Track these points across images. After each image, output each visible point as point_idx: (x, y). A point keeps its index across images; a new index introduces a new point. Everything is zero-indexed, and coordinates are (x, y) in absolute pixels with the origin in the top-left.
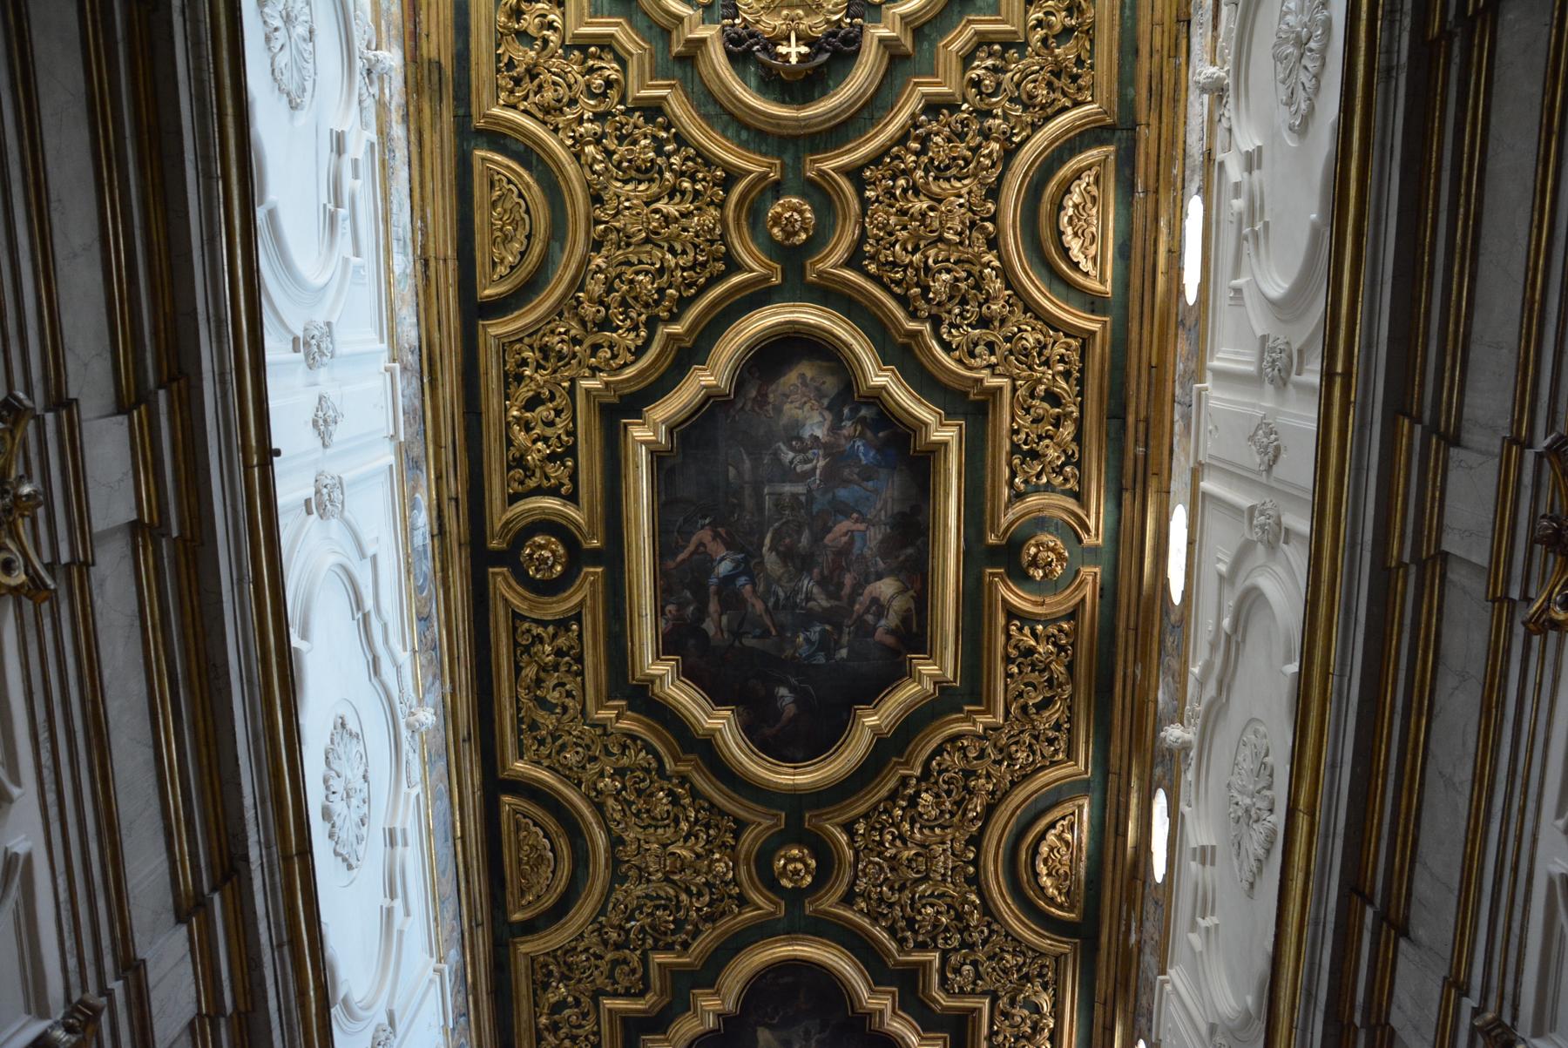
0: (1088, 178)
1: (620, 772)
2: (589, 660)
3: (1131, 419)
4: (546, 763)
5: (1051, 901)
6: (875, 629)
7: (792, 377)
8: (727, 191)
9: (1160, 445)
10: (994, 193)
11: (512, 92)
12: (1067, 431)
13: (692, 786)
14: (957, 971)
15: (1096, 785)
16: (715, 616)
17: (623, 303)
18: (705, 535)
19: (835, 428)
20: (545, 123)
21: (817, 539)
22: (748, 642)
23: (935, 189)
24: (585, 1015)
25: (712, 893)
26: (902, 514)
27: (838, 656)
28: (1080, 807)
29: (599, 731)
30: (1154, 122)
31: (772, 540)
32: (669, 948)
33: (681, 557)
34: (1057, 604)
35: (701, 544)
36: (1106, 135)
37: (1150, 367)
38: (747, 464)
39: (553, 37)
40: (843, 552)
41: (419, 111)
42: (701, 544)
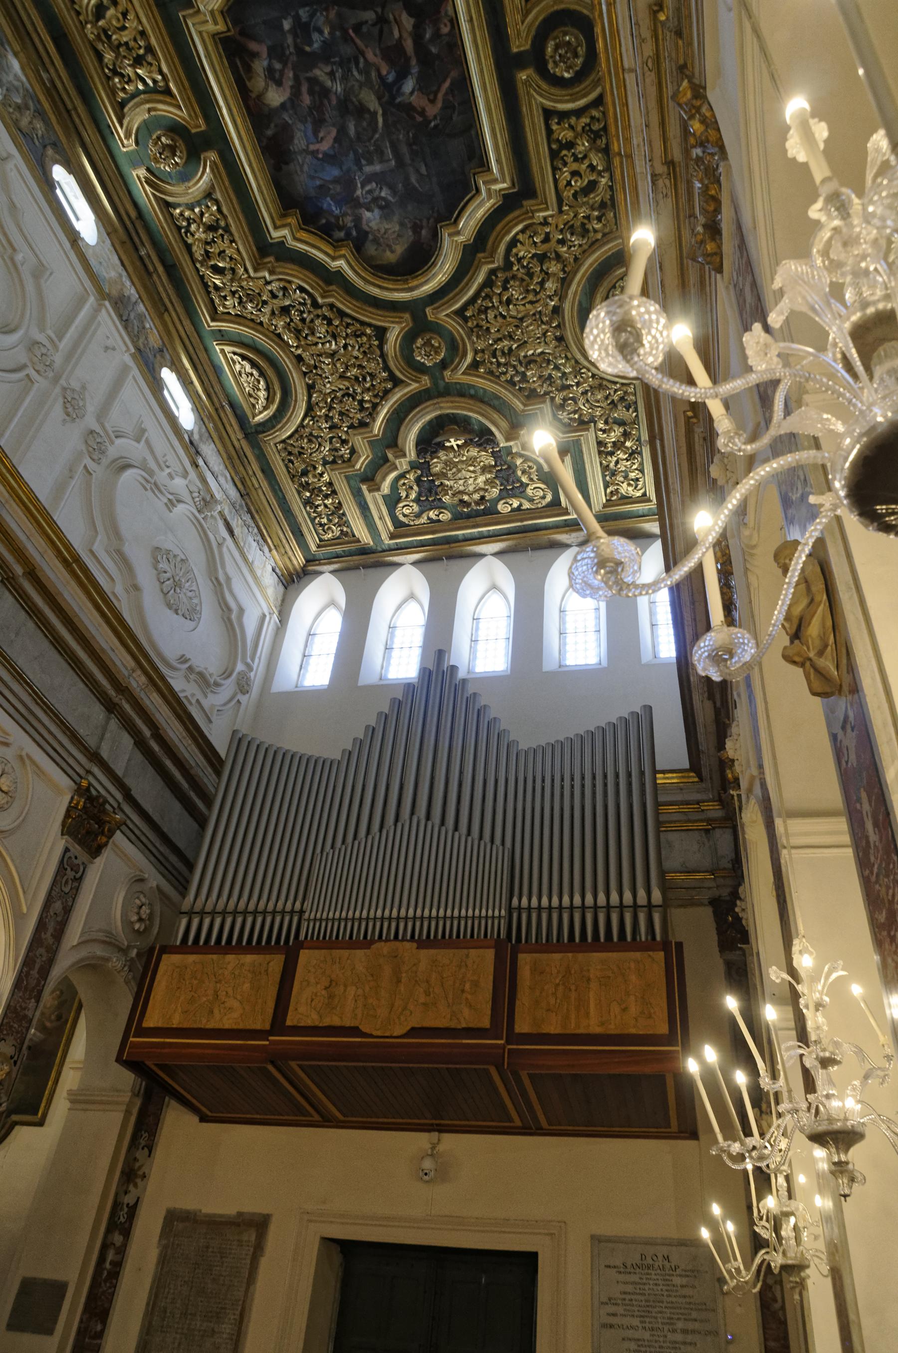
0: (259, 407)
3: (161, 269)
6: (269, 55)
7: (400, 249)
8: (474, 359)
9: (133, 263)
10: (310, 388)
11: (625, 392)
16: (405, 35)
17: (531, 275)
18: (432, 111)
19: (358, 220)
20: (602, 378)
22: (369, 16)
23: (347, 384)
26: (287, 163)
27: (290, 20)
31: (377, 122)
33: (447, 84)
34: (138, 116)
35: (432, 102)
36: (260, 429)
37: (167, 310)
38: (413, 179)
39: (601, 425)
40: (318, 123)
42: (432, 102)
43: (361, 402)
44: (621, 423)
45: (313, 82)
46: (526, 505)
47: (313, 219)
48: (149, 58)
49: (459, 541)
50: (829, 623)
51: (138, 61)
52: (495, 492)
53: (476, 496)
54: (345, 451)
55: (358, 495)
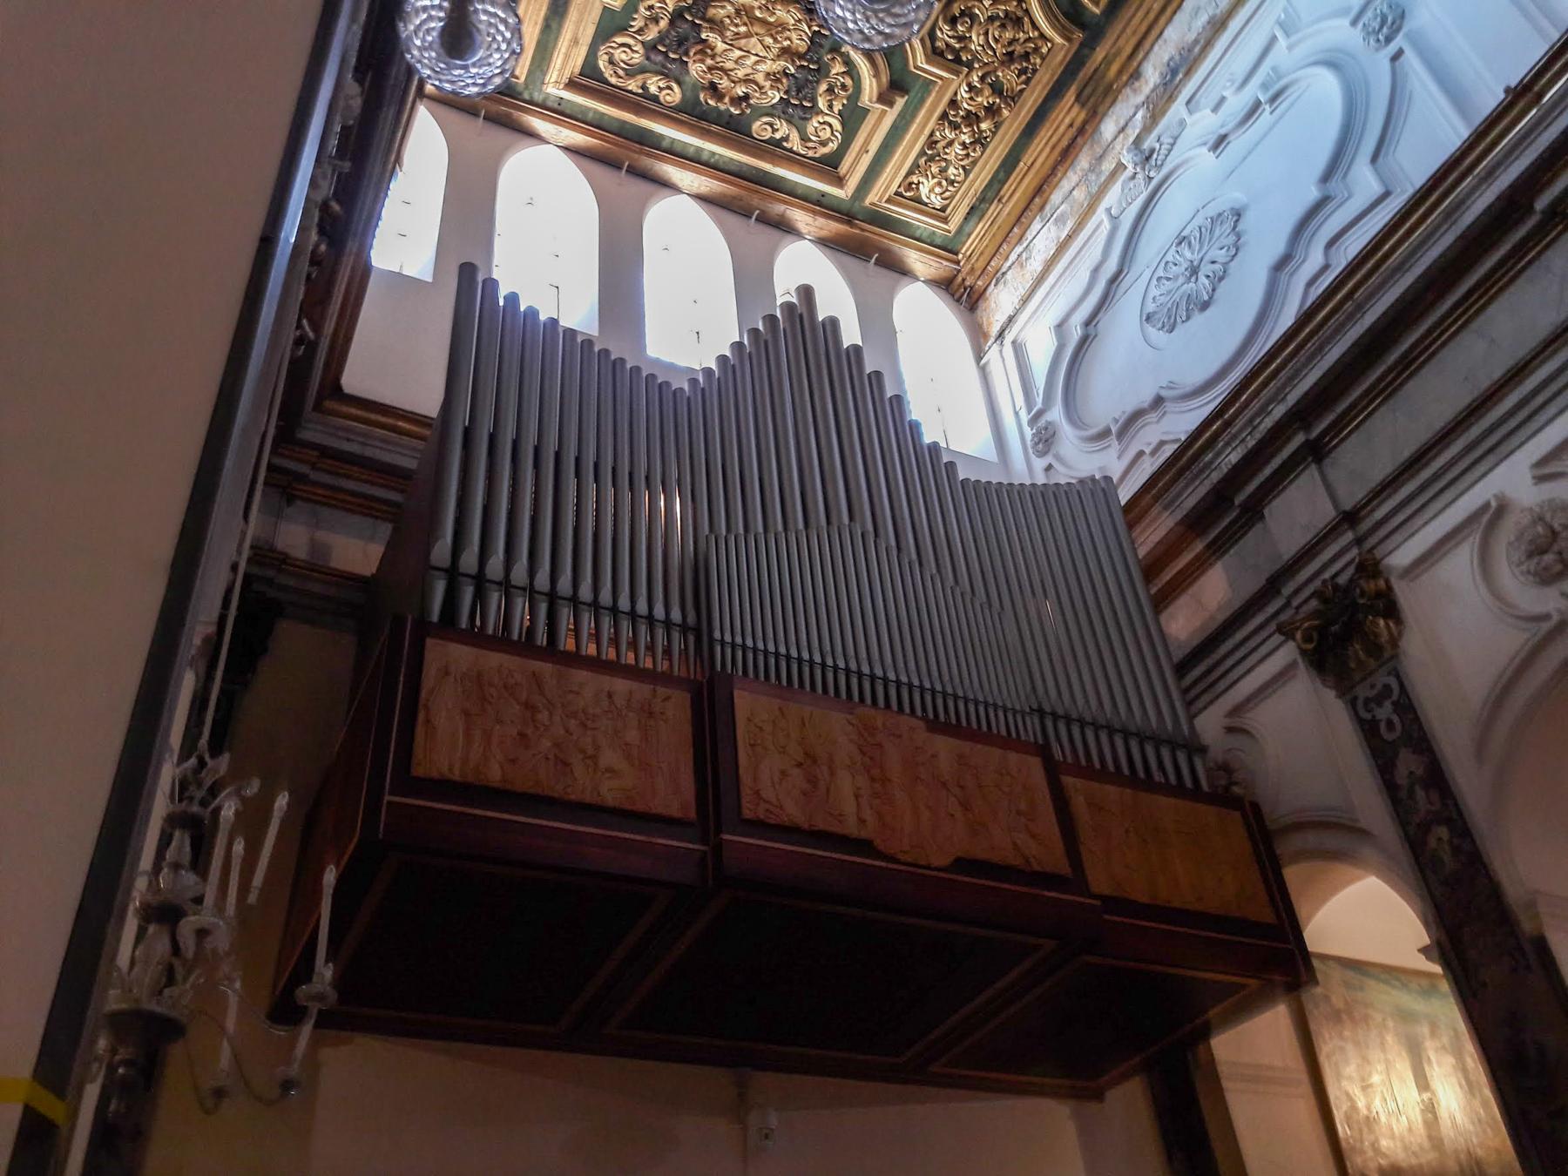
20: (1027, 11)
39: (975, 78)
41: (1120, 72)
44: (997, 89)
46: (795, 143)
52: (775, 97)
53: (740, 90)
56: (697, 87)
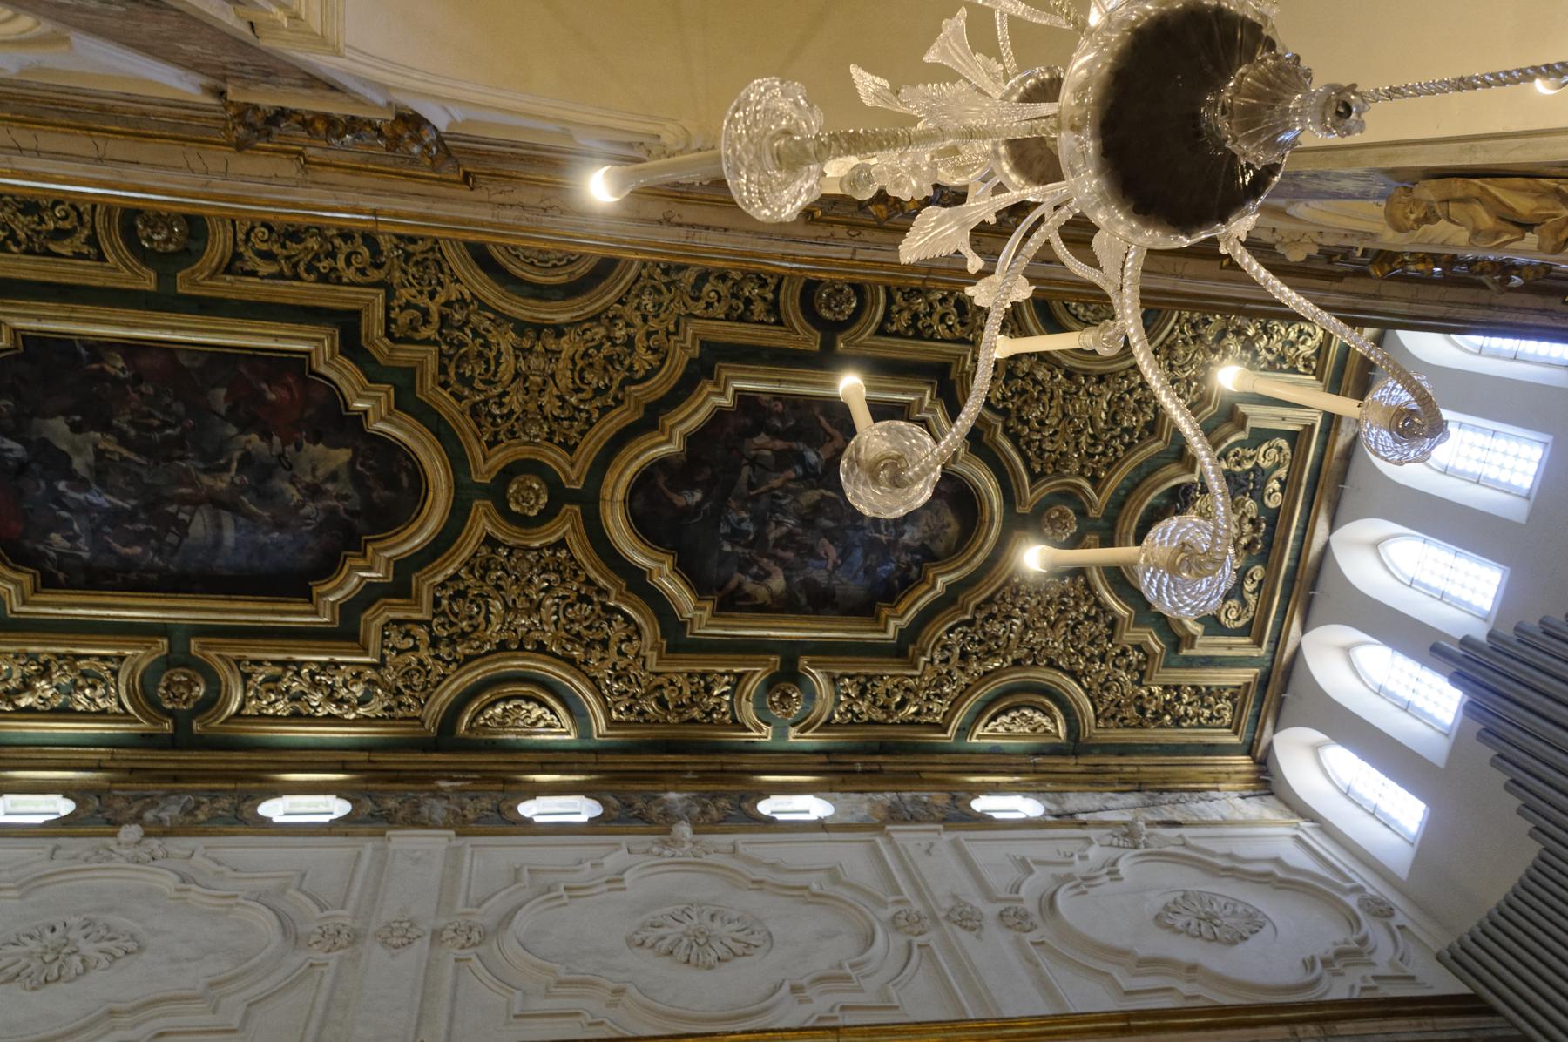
0: (1050, 727)
1: (630, 342)
2: (738, 327)
3: (880, 759)
4: (644, 273)
5: (481, 712)
7: (949, 518)
8: (1089, 479)
9: (864, 782)
10: (1051, 664)
11: (1188, 321)
12: (878, 715)
13: (612, 408)
14: (407, 634)
15: (587, 744)
17: (1024, 391)
21: (826, 533)
22: (746, 471)
24: (362, 271)
25: (502, 417)
26: (834, 596)
28: (568, 733)
29: (672, 328)
30: (1078, 769)
32: (443, 369)
33: (822, 419)
34: (748, 713)
37: (918, 772)
40: (812, 552)
43: (1087, 617)
45: (778, 543)
46: (1282, 473)
47: (890, 592)
48: (709, 679)
49: (1296, 567)
50: (1520, 182)
51: (708, 690)
52: (1250, 504)
53: (1247, 528)
54: (1134, 656)
55: (1190, 663)
56: (1249, 557)
